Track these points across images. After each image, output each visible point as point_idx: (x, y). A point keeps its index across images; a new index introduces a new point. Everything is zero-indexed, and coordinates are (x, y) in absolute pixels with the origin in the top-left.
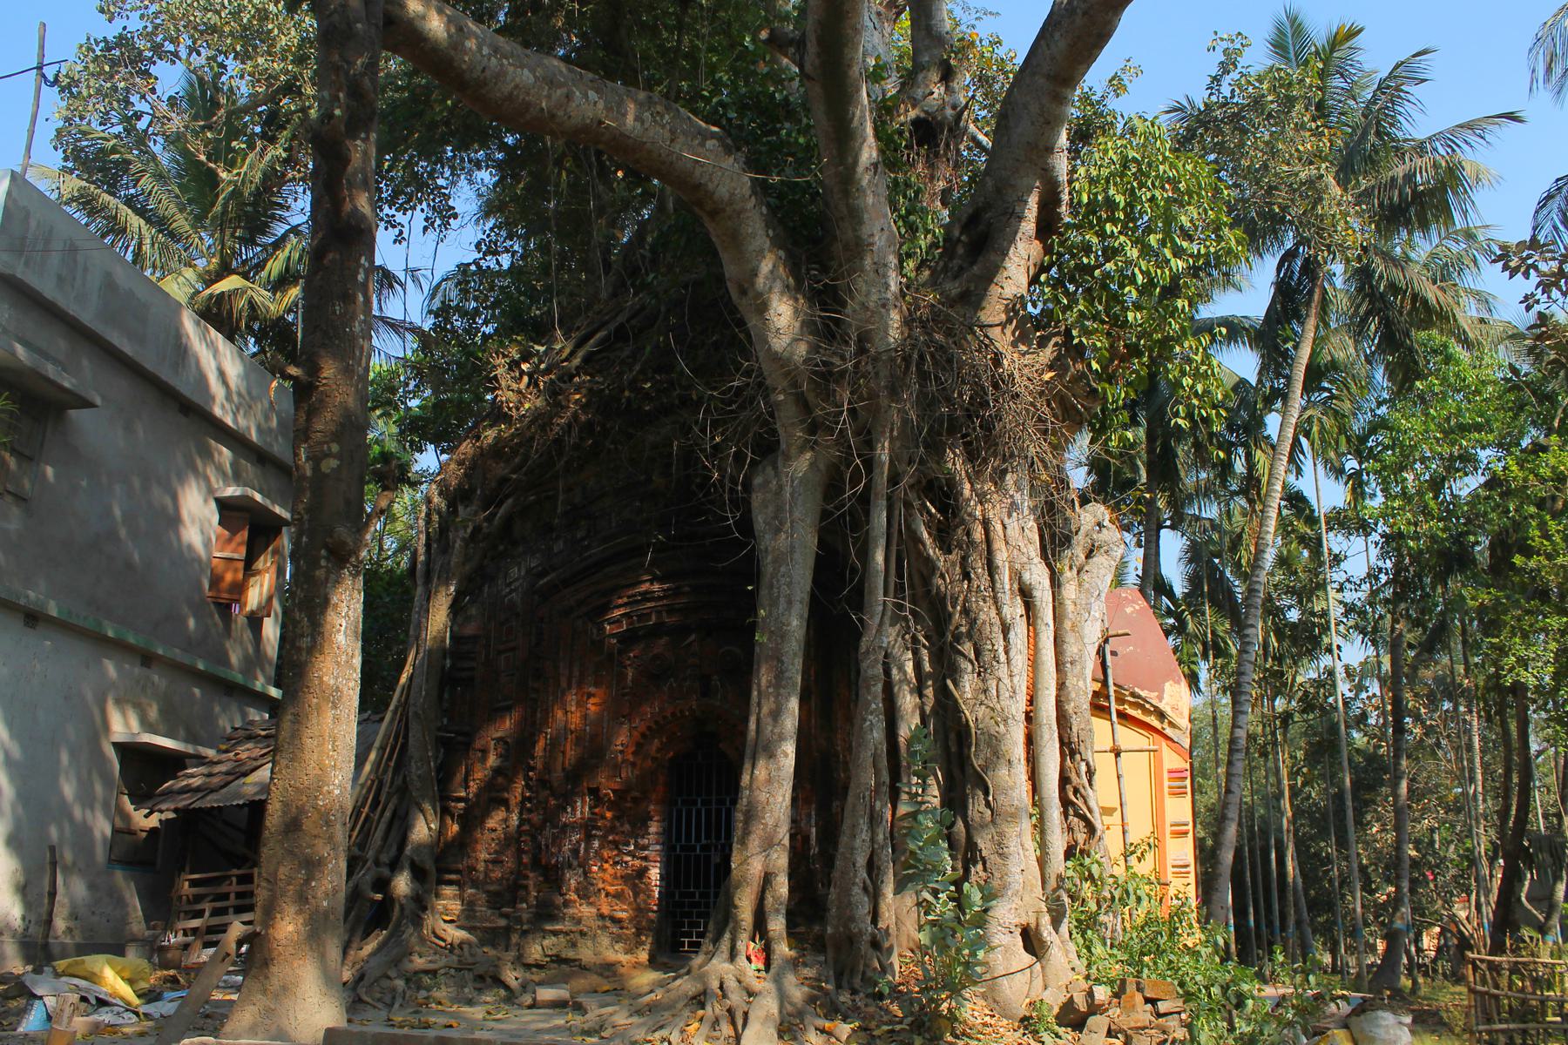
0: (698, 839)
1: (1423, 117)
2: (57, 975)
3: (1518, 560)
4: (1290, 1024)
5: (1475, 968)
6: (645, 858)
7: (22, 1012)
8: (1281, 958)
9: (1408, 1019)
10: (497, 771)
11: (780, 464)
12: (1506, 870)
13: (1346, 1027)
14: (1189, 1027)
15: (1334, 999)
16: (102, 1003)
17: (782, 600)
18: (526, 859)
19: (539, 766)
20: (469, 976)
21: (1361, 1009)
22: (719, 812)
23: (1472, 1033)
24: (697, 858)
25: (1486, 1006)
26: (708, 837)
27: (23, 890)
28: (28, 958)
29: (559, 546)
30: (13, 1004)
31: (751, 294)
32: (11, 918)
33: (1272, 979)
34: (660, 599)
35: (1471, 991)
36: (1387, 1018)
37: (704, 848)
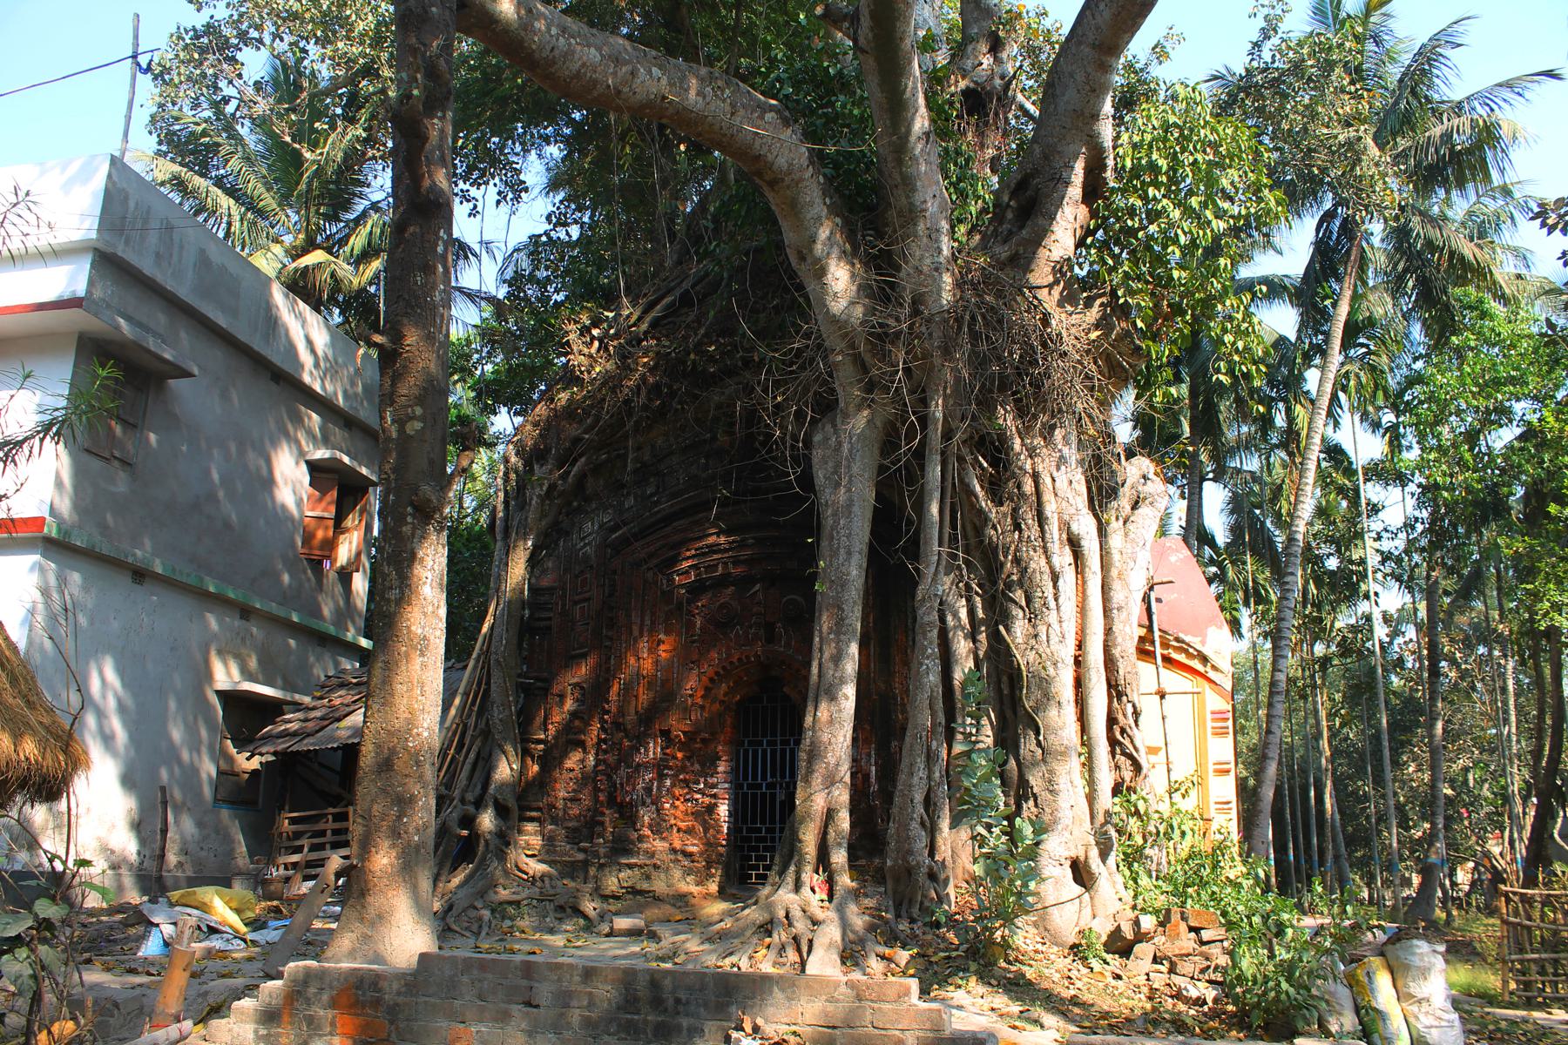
0: (764, 778)
1: (1457, 81)
2: (172, 905)
3: (1553, 509)
4: (1328, 952)
5: (1508, 900)
6: (714, 796)
7: (143, 938)
8: (1320, 889)
9: (1442, 948)
10: (574, 715)
11: (839, 421)
12: (1538, 807)
13: (1382, 954)
14: (1231, 953)
15: (1370, 928)
16: (213, 930)
17: (842, 551)
18: (602, 797)
19: (614, 709)
20: (550, 907)
21: (1396, 938)
22: (783, 752)
23: (1504, 962)
24: (764, 795)
25: (1518, 937)
27: (137, 826)
28: (144, 891)
30: (132, 931)
31: (809, 261)
32: (127, 853)
33: (1312, 911)
34: (726, 550)
35: (1504, 922)
36: (1422, 947)
37: (769, 786)
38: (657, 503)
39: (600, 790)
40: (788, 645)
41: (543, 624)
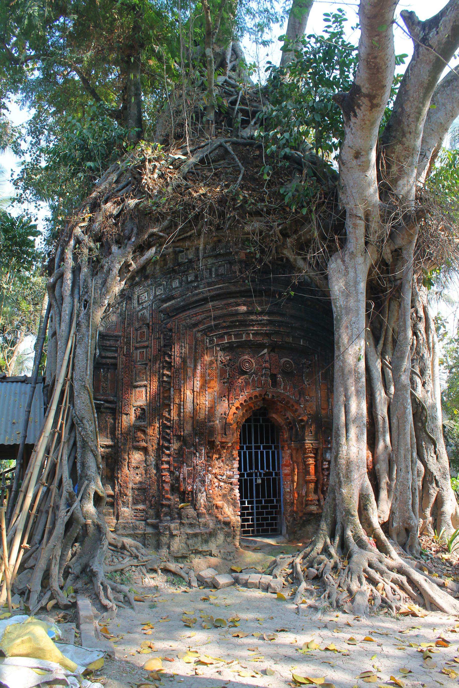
6: (231, 483)
11: (347, 259)
18: (167, 487)
19: (176, 426)
22: (256, 453)
26: (251, 468)
29: (176, 284)
31: (362, 159)
37: (249, 475)
38: (196, 288)
39: (164, 482)
40: (285, 389)
41: (108, 361)
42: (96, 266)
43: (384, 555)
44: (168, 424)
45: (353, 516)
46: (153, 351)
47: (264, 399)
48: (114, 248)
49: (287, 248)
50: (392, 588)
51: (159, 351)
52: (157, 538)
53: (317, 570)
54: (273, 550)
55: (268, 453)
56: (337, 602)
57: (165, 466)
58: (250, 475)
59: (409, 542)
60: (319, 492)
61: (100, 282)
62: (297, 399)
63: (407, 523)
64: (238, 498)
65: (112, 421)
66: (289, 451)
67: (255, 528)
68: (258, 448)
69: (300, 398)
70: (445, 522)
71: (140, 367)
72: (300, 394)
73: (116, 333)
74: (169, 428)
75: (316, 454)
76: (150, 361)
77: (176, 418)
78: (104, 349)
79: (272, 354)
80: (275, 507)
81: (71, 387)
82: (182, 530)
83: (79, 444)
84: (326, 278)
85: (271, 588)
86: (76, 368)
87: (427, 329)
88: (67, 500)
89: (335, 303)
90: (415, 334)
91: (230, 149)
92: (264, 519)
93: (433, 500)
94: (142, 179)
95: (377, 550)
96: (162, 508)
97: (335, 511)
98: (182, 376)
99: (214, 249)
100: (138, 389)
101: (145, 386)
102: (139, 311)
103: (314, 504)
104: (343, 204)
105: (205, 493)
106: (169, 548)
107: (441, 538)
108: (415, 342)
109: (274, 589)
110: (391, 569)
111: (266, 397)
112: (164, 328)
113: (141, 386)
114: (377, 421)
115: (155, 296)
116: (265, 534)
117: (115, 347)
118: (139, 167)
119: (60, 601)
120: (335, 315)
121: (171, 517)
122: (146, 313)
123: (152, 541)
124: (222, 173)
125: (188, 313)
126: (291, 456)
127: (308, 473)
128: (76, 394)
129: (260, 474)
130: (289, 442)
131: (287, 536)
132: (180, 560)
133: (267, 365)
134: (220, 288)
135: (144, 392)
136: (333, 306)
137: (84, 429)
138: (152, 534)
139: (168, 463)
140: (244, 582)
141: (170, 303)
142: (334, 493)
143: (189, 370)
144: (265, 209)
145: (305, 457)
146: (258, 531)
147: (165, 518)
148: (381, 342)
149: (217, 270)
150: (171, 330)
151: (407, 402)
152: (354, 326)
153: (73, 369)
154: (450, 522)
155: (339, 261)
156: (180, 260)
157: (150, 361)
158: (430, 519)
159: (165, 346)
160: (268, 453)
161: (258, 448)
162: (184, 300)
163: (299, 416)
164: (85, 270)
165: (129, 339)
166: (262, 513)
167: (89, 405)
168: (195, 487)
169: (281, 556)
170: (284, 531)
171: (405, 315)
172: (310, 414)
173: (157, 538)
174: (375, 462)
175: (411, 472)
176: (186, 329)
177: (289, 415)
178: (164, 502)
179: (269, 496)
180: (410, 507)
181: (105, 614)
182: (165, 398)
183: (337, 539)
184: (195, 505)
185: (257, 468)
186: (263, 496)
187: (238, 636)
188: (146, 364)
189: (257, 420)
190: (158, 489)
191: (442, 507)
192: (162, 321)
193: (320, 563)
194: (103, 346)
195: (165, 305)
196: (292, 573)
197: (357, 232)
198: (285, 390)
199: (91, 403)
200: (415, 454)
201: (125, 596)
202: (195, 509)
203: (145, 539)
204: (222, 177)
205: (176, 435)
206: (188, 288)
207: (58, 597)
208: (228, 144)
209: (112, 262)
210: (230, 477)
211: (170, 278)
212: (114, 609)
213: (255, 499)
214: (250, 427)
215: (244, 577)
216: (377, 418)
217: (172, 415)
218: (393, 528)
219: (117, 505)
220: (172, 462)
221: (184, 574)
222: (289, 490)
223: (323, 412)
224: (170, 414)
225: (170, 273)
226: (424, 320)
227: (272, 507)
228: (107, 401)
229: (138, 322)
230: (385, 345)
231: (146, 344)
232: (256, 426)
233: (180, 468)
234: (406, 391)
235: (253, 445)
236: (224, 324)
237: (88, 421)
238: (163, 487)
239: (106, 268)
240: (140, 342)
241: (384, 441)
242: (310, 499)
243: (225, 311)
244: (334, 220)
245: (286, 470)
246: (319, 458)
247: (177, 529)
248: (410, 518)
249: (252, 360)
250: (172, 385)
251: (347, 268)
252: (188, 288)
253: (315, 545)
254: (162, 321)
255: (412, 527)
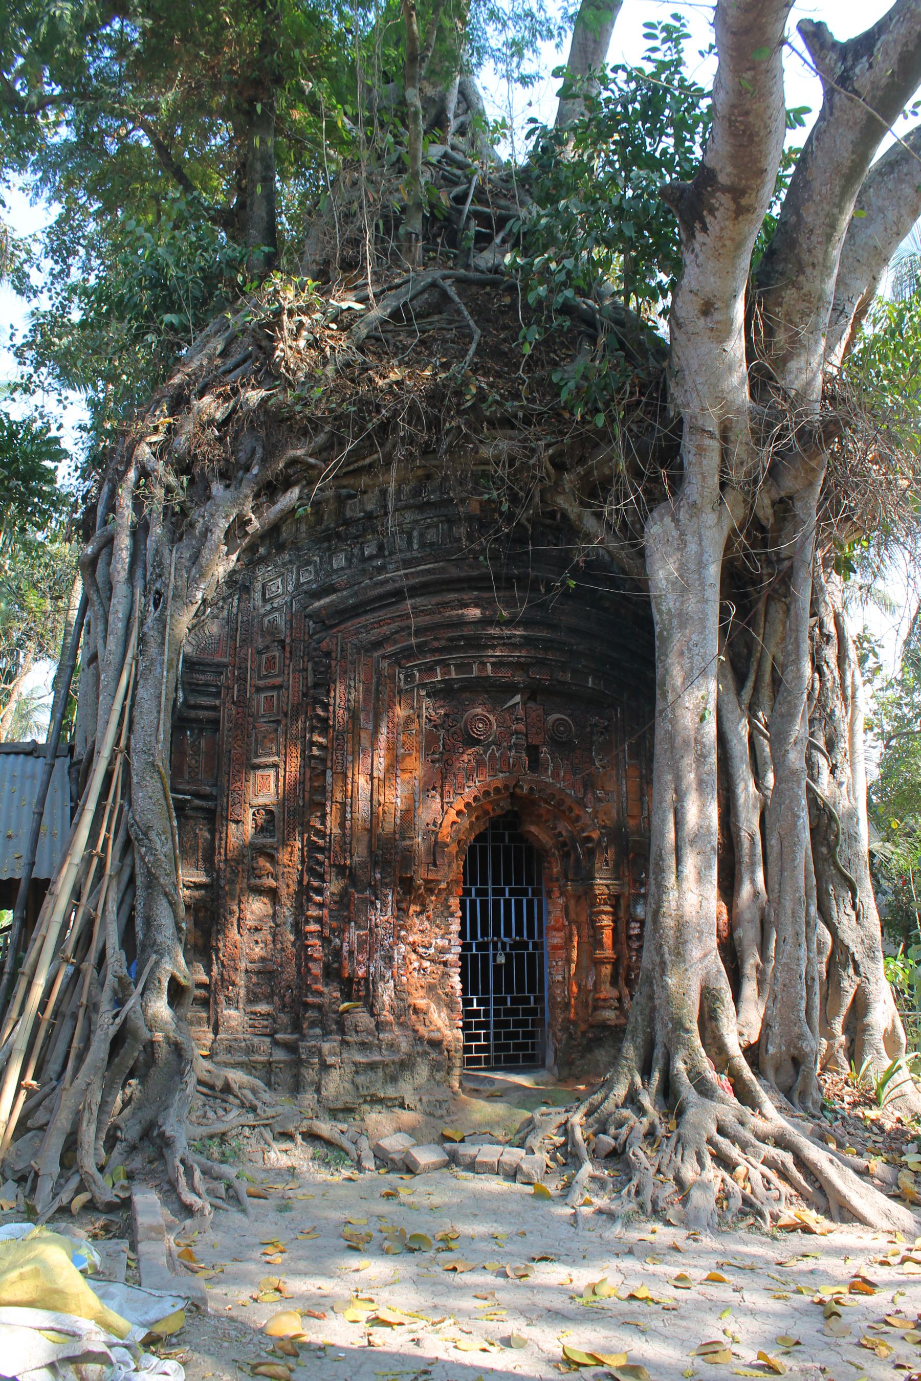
6: (445, 963)
11: (683, 515)
18: (316, 969)
19: (335, 847)
22: (496, 904)
26: (485, 933)
29: (339, 561)
31: (717, 316)
38: (381, 569)
39: (310, 958)
40: (555, 775)
41: (202, 714)
42: (179, 522)
43: (748, 1110)
44: (321, 842)
45: (687, 1031)
46: (292, 696)
47: (512, 795)
48: (217, 488)
49: (564, 493)
50: (763, 1176)
51: (304, 695)
52: (295, 1071)
53: (616, 1138)
54: (526, 1098)
55: (519, 904)
56: (654, 1202)
57: (313, 927)
58: (482, 947)
59: (799, 1085)
60: (621, 982)
61: (187, 555)
62: (580, 795)
63: (796, 1047)
64: (459, 993)
65: (207, 835)
66: (561, 901)
67: (492, 1054)
68: (499, 892)
69: (585, 794)
70: (871, 1045)
71: (264, 728)
72: (585, 786)
73: (218, 659)
74: (321, 850)
75: (616, 906)
76: (286, 715)
77: (336, 831)
78: (193, 691)
79: (531, 704)
80: (533, 1011)
81: (127, 765)
82: (345, 1055)
83: (140, 881)
84: (641, 554)
85: (522, 1173)
86: (137, 727)
87: (842, 658)
88: (115, 992)
89: (658, 604)
90: (817, 668)
91: (452, 291)
92: (509, 1036)
93: (848, 1000)
94: (275, 348)
95: (736, 1101)
96: (306, 1011)
97: (651, 1021)
98: (349, 747)
99: (417, 492)
100: (260, 772)
101: (275, 766)
102: (265, 615)
103: (609, 1007)
104: (676, 405)
105: (392, 983)
106: (318, 1091)
107: (864, 1078)
108: (817, 685)
109: (528, 1175)
110: (763, 1139)
111: (518, 790)
112: (315, 649)
113: (266, 766)
114: (739, 842)
115: (298, 585)
116: (511, 1065)
117: (216, 686)
118: (270, 326)
119: (97, 1195)
120: (657, 629)
121: (323, 1029)
122: (280, 619)
123: (285, 1077)
124: (436, 340)
125: (362, 620)
126: (566, 909)
127: (599, 944)
128: (135, 780)
129: (504, 944)
130: (562, 882)
131: (556, 1070)
132: (340, 1115)
133: (521, 727)
134: (428, 571)
135: (272, 778)
136: (654, 610)
137: (151, 850)
138: (284, 1062)
139: (319, 920)
140: (468, 1160)
141: (327, 600)
142: (651, 985)
143: (363, 735)
144: (520, 414)
145: (593, 913)
146: (497, 1059)
147: (311, 1032)
148: (750, 684)
149: (422, 535)
150: (328, 654)
151: (799, 805)
152: (696, 650)
153: (130, 730)
154: (882, 1046)
155: (668, 520)
156: (349, 514)
157: (286, 715)
158: (842, 1039)
159: (316, 686)
160: (519, 904)
161: (499, 892)
162: (356, 593)
163: (583, 830)
164: (157, 530)
165: (243, 670)
166: (506, 1024)
167: (162, 802)
168: (372, 970)
169: (544, 1109)
170: (550, 1060)
171: (797, 631)
172: (604, 827)
173: (295, 1071)
174: (733, 923)
175: (804, 946)
176: (359, 653)
177: (563, 827)
178: (310, 999)
179: (520, 989)
180: (803, 1015)
181: (188, 1222)
182: (314, 790)
183: (656, 1076)
184: (373, 1005)
185: (497, 933)
186: (509, 990)
187: (454, 1269)
188: (278, 722)
189: (498, 838)
190: (299, 972)
191: (865, 1015)
192: (311, 636)
193: (620, 1125)
194: (190, 684)
195: (317, 604)
196: (565, 1144)
197: (705, 462)
198: (555, 778)
199: (166, 798)
200: (813, 909)
201: (229, 1187)
202: (372, 1015)
203: (270, 1072)
204: (435, 348)
205: (335, 865)
206: (364, 570)
207: (93, 1187)
208: (449, 282)
209: (212, 515)
210: (443, 951)
211: (329, 549)
212: (207, 1212)
213: (492, 996)
214: (484, 851)
215: (467, 1150)
216: (739, 836)
217: (328, 824)
218: (768, 1057)
219: (216, 1003)
220: (327, 919)
221: (347, 1145)
222: (560, 978)
223: (632, 823)
224: (323, 823)
225: (327, 540)
226: (836, 641)
227: (527, 1012)
228: (197, 795)
229: (263, 636)
230: (756, 689)
231: (278, 681)
232: (496, 850)
233: (343, 931)
234: (798, 782)
235: (490, 887)
236: (436, 644)
237: (158, 835)
238: (309, 969)
239: (199, 526)
240: (266, 677)
241: (753, 881)
242: (602, 996)
243: (437, 618)
244: (659, 439)
245: (556, 939)
246: (622, 915)
247: (335, 1054)
248: (801, 1037)
249: (491, 717)
250: (329, 764)
251: (682, 534)
252: (364, 570)
253: (611, 1089)
254: (311, 636)
255: (806, 1055)
